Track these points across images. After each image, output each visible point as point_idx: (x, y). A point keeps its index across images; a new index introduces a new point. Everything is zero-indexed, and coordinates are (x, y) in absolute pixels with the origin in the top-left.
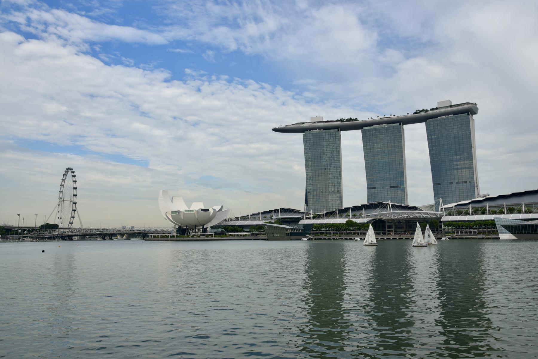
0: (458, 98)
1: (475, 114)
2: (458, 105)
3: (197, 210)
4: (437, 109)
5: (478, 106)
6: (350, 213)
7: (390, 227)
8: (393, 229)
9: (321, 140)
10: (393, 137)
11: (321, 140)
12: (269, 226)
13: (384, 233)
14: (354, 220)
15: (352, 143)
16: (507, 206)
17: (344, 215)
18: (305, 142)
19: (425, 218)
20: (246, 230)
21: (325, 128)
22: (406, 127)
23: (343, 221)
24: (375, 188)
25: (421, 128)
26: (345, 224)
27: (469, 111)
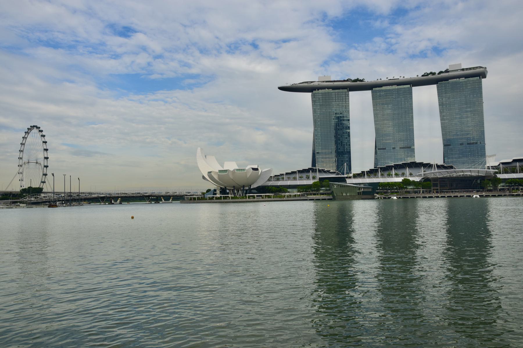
0: (466, 62)
1: (484, 77)
2: (470, 69)
3: (232, 169)
4: (447, 71)
5: (487, 69)
6: (393, 172)
7: (435, 185)
8: (439, 188)
9: (329, 98)
10: (403, 99)
11: (329, 98)
12: (339, 185)
13: (430, 192)
14: (411, 179)
15: (360, 104)
16: (520, 166)
17: (386, 173)
18: (314, 102)
19: (465, 177)
20: (289, 190)
21: (334, 88)
22: (414, 89)
23: (400, 180)
24: (385, 149)
25: (433, 88)
26: (400, 182)
27: (483, 75)
